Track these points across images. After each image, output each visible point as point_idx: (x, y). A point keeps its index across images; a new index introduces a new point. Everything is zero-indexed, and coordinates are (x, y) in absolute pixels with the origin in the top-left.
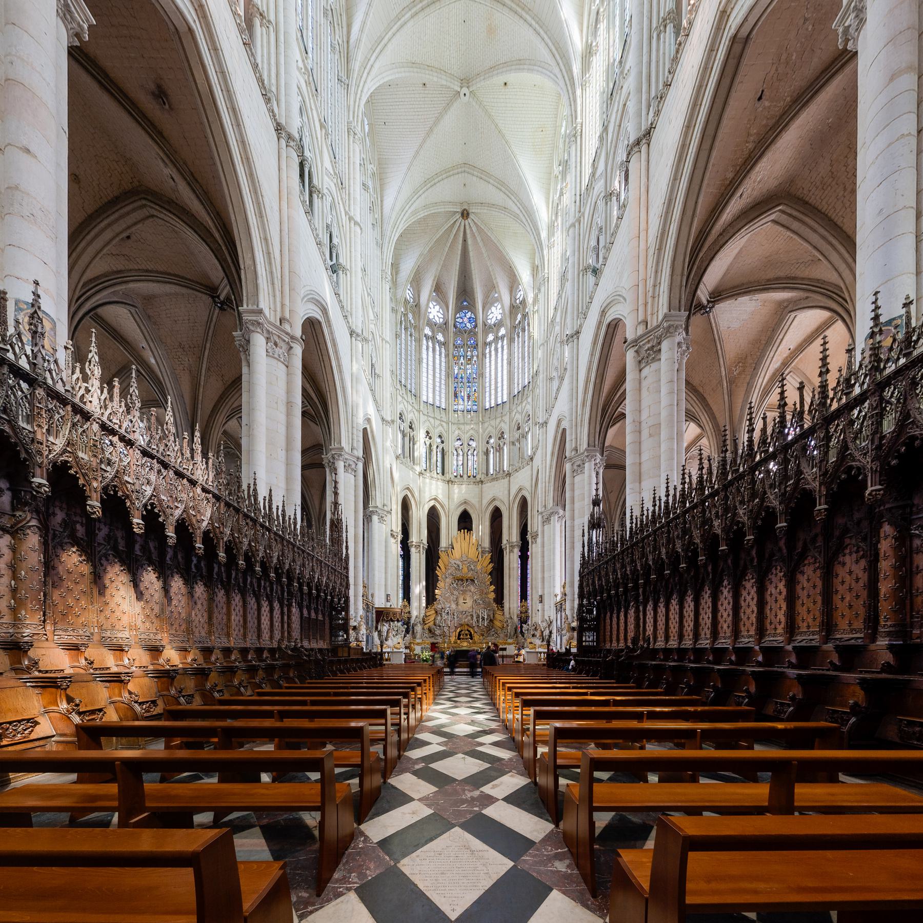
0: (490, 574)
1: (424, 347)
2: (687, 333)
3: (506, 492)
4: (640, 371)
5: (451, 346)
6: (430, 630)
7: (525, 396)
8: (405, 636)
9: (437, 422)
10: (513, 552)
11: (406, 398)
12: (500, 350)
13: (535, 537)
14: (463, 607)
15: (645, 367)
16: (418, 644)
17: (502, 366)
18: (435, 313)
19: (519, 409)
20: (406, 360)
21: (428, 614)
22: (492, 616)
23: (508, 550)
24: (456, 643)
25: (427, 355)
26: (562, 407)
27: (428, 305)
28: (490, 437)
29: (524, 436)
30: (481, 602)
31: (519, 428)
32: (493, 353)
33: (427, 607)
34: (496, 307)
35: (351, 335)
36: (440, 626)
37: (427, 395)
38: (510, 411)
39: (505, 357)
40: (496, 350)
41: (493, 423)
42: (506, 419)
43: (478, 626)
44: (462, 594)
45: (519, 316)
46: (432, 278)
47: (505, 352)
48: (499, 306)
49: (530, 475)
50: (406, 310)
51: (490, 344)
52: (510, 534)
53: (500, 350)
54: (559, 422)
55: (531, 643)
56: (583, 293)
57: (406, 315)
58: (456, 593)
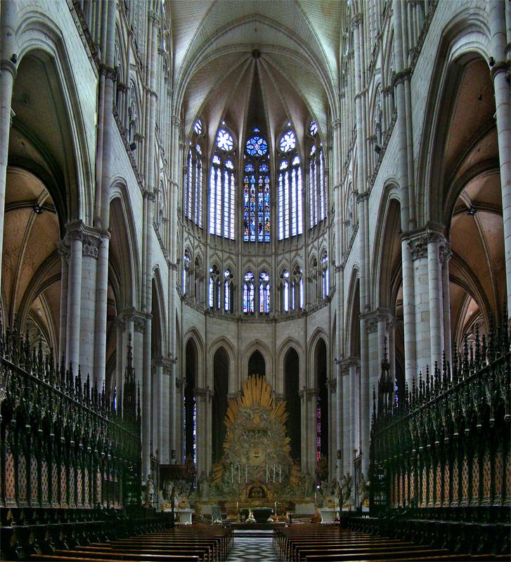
0: (285, 424)
1: (212, 177)
2: (448, 239)
4: (413, 261)
5: (241, 174)
6: (217, 487)
7: (321, 232)
8: (190, 495)
9: (226, 255)
10: (311, 400)
11: (192, 234)
12: (294, 179)
13: (334, 386)
14: (257, 462)
15: (416, 259)
16: (205, 503)
17: (297, 201)
18: (225, 141)
19: (316, 243)
20: (193, 193)
21: (215, 470)
22: (287, 471)
23: (305, 398)
24: (246, 502)
25: (216, 184)
26: (355, 258)
27: (217, 136)
28: (284, 271)
29: (321, 274)
30: (275, 456)
31: (315, 265)
32: (287, 182)
33: (213, 462)
34: (290, 135)
35: (144, 197)
36: (228, 483)
37: (214, 228)
38: (306, 246)
39: (300, 187)
40: (290, 179)
41: (287, 256)
43: (272, 482)
44: (254, 447)
45: (314, 149)
46: (222, 110)
47: (300, 182)
48: (292, 136)
49: (328, 317)
50: (194, 143)
51: (283, 172)
52: (307, 378)
53: (294, 179)
54: (387, 189)
55: (330, 501)
56: (370, 159)
57: (194, 149)
58: (246, 445)
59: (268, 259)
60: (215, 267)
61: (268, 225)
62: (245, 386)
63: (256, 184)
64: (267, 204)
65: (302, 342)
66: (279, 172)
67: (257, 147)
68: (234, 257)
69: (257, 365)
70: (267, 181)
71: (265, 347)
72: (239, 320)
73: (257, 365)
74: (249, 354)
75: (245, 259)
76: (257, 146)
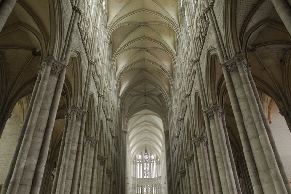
67: (146, 157)
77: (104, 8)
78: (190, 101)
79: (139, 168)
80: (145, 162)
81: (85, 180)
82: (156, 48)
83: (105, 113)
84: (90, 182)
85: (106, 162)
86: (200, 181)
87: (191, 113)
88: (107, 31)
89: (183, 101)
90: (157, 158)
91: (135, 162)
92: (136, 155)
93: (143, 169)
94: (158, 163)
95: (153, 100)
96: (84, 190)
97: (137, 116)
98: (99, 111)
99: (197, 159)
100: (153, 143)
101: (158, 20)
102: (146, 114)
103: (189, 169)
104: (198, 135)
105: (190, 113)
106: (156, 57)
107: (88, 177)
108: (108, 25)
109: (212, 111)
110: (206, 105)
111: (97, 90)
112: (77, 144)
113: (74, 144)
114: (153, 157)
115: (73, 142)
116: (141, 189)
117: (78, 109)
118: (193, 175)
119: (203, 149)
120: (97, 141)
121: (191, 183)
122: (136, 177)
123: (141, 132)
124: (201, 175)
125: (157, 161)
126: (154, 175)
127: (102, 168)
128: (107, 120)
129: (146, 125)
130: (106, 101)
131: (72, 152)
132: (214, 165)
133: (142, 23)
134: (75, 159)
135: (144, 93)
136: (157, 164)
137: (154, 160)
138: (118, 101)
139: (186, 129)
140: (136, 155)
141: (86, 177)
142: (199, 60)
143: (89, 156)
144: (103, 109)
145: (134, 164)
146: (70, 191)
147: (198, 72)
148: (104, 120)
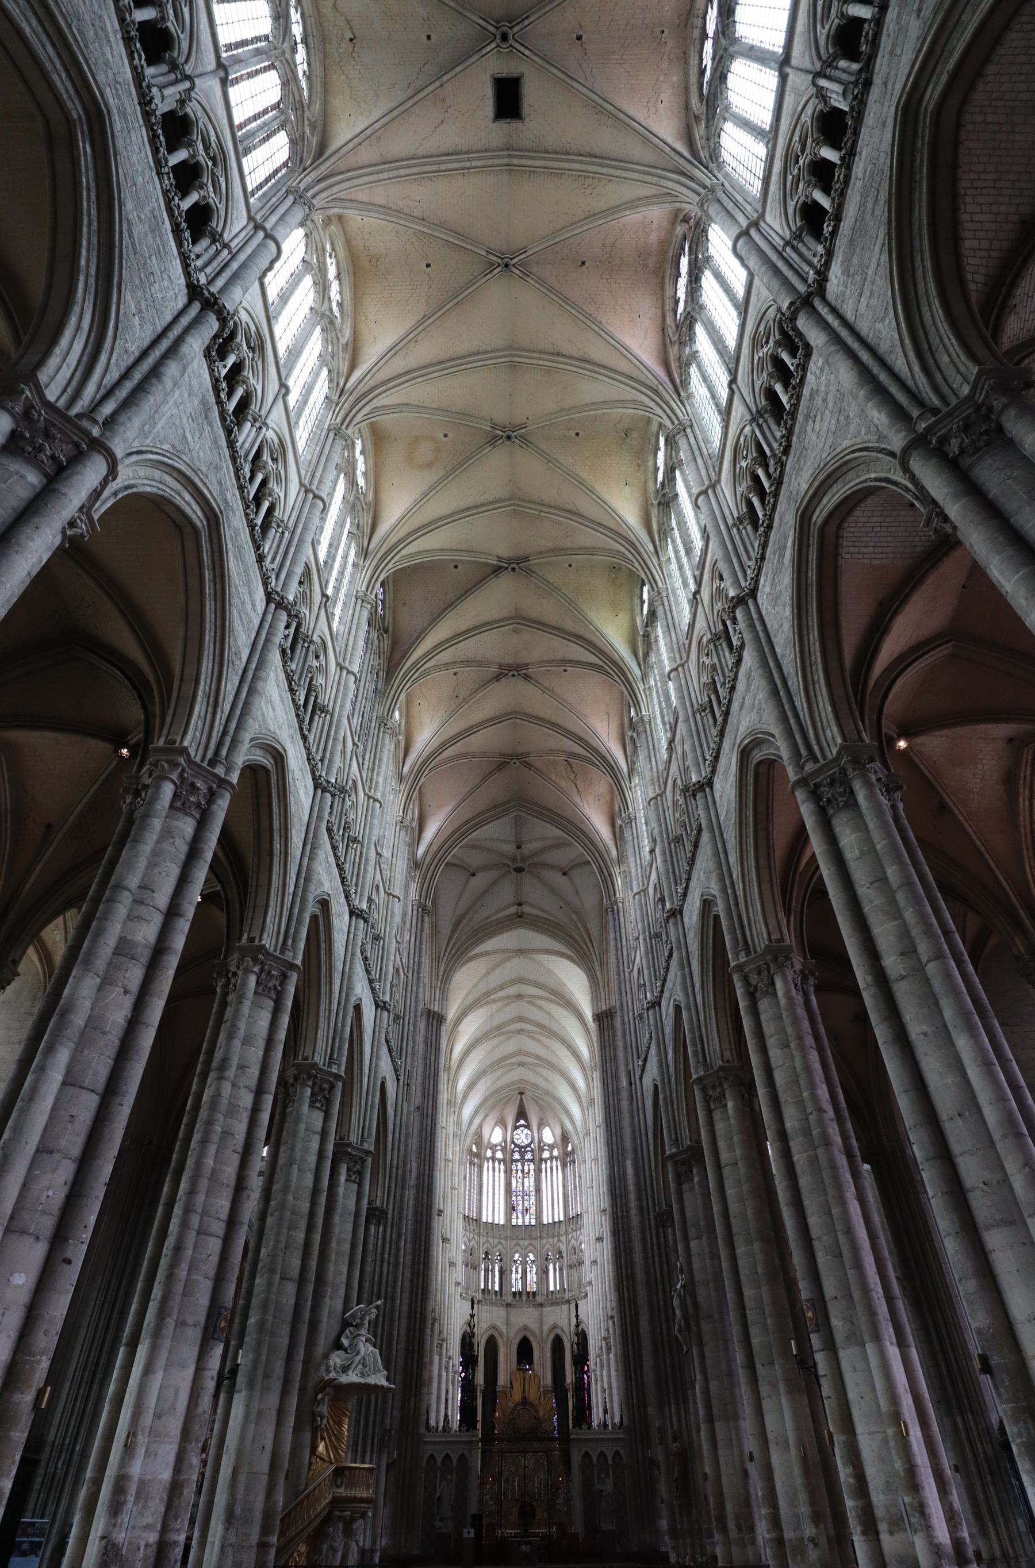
3: (566, 1320)
41: (550, 1240)
42: (563, 1239)
51: (546, 1161)
59: (534, 1242)
60: (487, 1253)
61: (534, 1208)
62: (513, 1377)
63: (523, 1171)
64: (532, 1189)
65: (566, 1329)
66: (541, 1160)
67: (522, 1137)
68: (503, 1241)
69: (525, 1350)
70: (532, 1167)
71: (533, 1333)
72: (508, 1305)
73: (525, 1350)
74: (517, 1341)
75: (513, 1243)
76: (523, 1136)
77: (361, 481)
78: (711, 806)
79: (493, 1178)
80: (517, 1156)
81: (212, 1148)
82: (567, 662)
83: (343, 879)
84: (235, 1159)
85: (338, 1092)
86: (786, 1153)
87: (720, 854)
88: (371, 563)
89: (678, 839)
90: (565, 1138)
91: (478, 1155)
92: (480, 1126)
93: (508, 1184)
94: (567, 1159)
95: (554, 891)
96: (200, 1198)
97: (492, 957)
98: (311, 845)
99: (763, 1050)
100: (544, 1072)
101: (567, 543)
102: (520, 952)
103: (720, 1127)
104: (761, 943)
105: (717, 854)
106: (563, 703)
107: (226, 1134)
108: (371, 547)
109: (843, 771)
110: (804, 752)
111: (308, 754)
112: (158, 919)
113: (142, 910)
114: (548, 1136)
115: (138, 902)
116: (502, 1272)
117: (189, 760)
118: (738, 1152)
119: (790, 999)
120: (292, 966)
121: (730, 1192)
122: (478, 1221)
123: (499, 1027)
124: (788, 1125)
125: (566, 1154)
126: (552, 1212)
127: (317, 1119)
128: (352, 913)
129: (519, 997)
130: (355, 840)
131: (124, 948)
132: (885, 1019)
133: (509, 561)
134: (134, 985)
135: (514, 860)
136: (564, 1165)
137: (551, 1147)
138: (410, 877)
139: (694, 947)
140: (480, 1126)
141: (218, 1129)
142: (753, 592)
143: (241, 1032)
144: (337, 857)
145: (472, 1163)
146: (76, 1151)
147: (757, 638)
148: (341, 920)
